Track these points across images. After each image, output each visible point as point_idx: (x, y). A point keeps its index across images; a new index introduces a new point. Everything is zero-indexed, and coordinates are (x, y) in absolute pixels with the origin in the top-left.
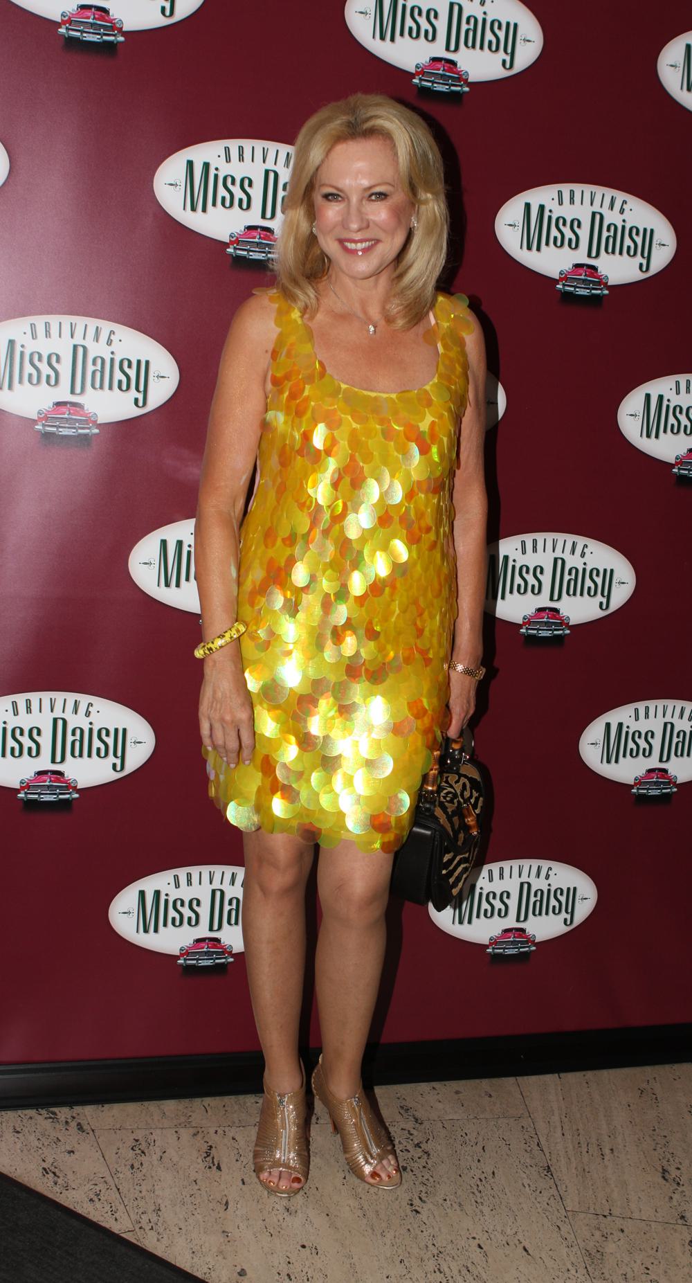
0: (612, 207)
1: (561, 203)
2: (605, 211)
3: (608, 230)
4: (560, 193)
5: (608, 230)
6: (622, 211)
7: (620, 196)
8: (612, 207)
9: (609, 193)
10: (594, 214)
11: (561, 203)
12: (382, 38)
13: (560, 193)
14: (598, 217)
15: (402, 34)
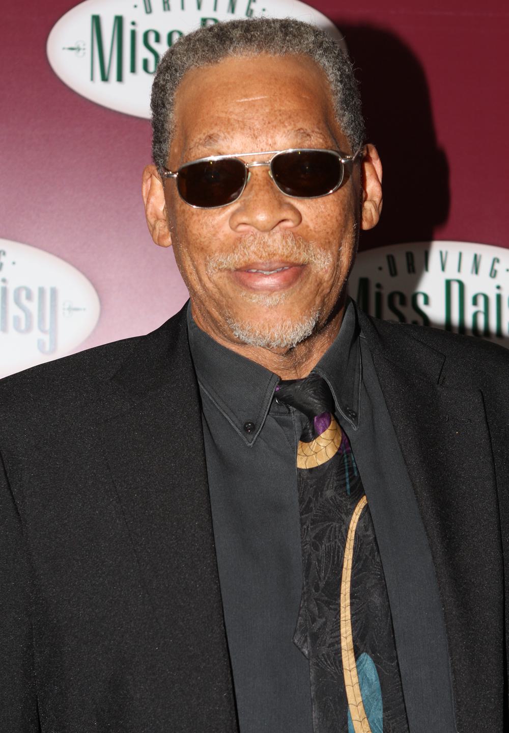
0: (476, 269)
1: (393, 272)
2: (466, 276)
3: (475, 302)
4: (391, 260)
5: (475, 302)
6: (493, 274)
7: (488, 252)
8: (476, 269)
9: (469, 250)
10: (448, 284)
11: (393, 272)
12: (105, 78)
13: (391, 260)
14: (455, 288)
15: (133, 70)
